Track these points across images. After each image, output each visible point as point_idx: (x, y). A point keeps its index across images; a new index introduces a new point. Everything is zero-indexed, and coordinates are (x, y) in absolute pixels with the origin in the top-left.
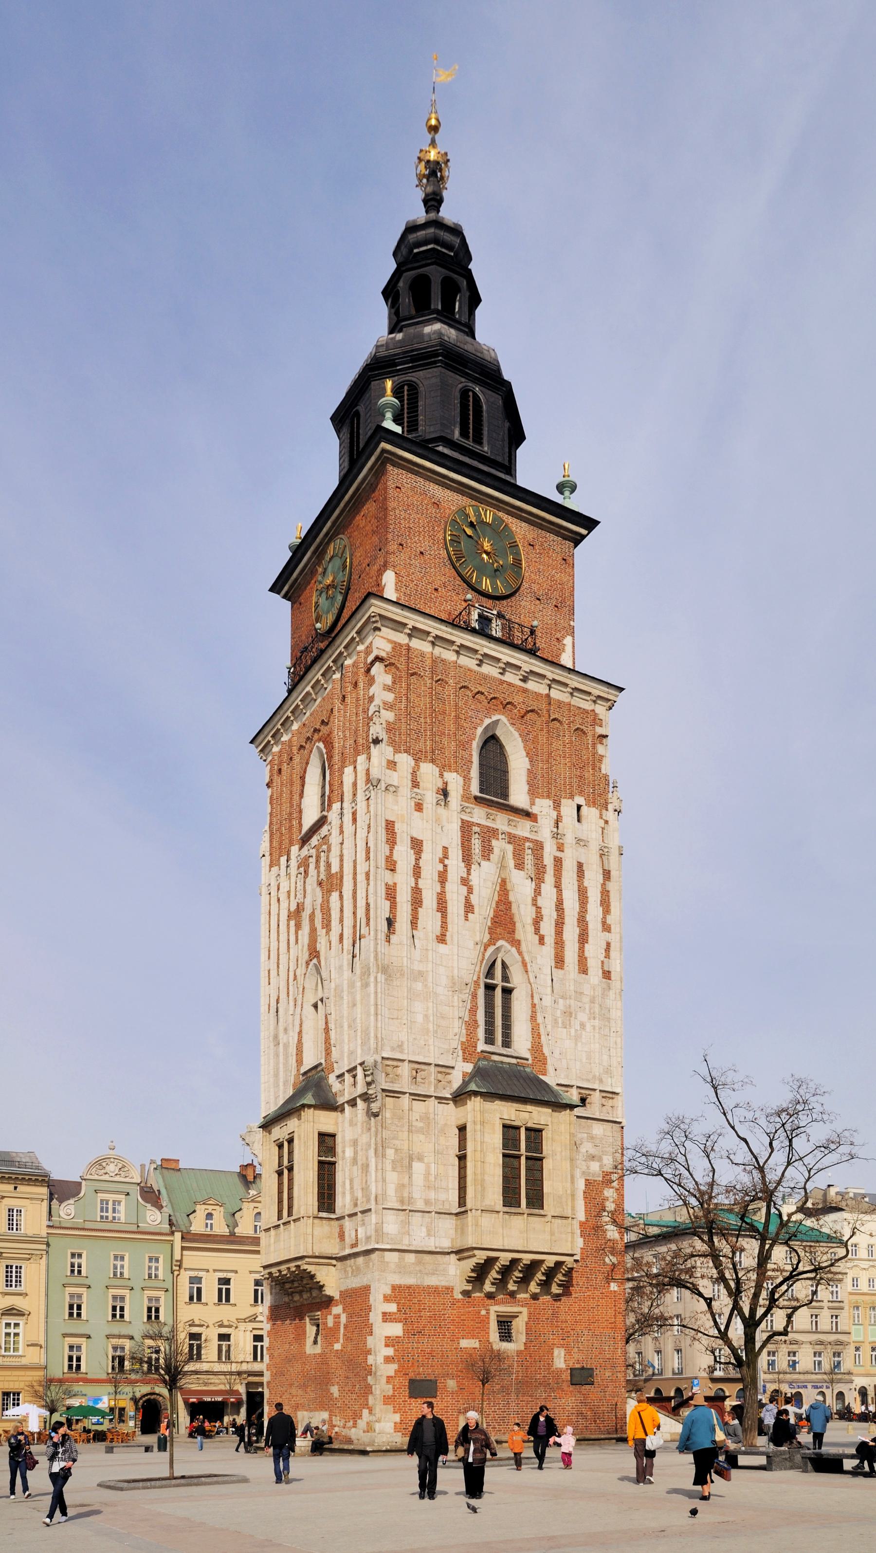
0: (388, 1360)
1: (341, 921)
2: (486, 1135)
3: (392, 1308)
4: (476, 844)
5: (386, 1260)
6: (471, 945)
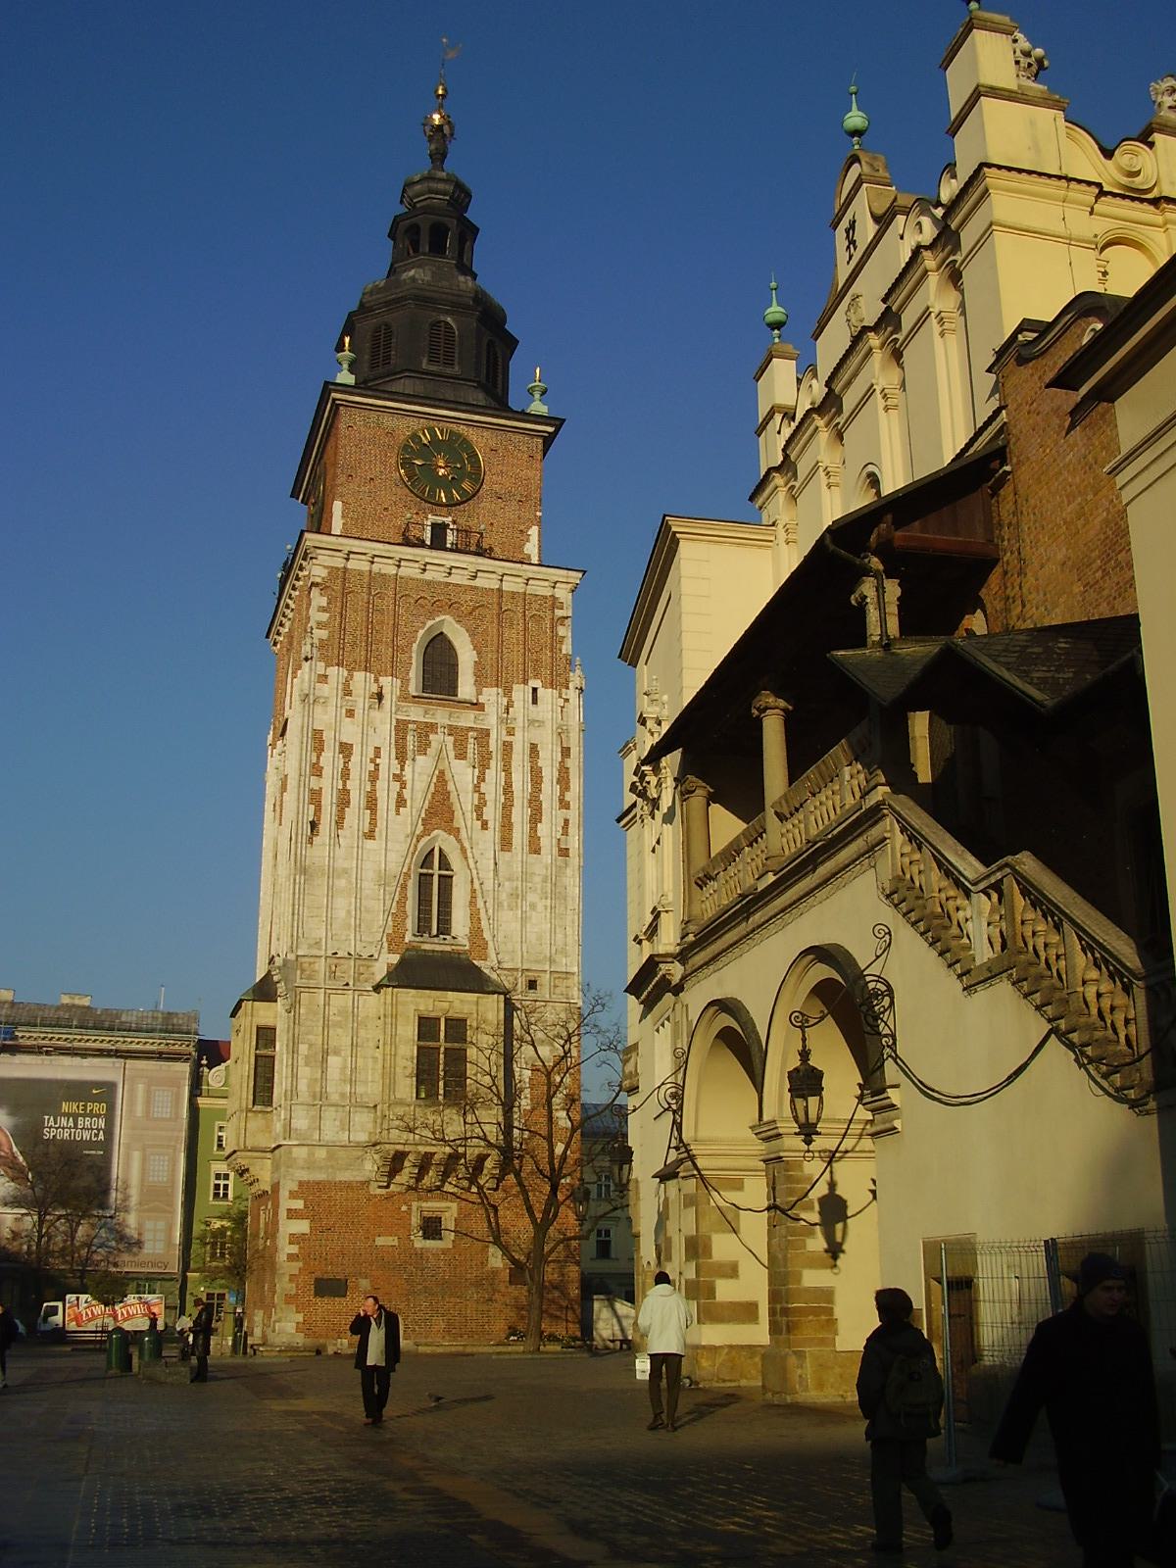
0: (291, 1257)
2: (398, 1027)
3: (299, 1204)
5: (294, 1155)
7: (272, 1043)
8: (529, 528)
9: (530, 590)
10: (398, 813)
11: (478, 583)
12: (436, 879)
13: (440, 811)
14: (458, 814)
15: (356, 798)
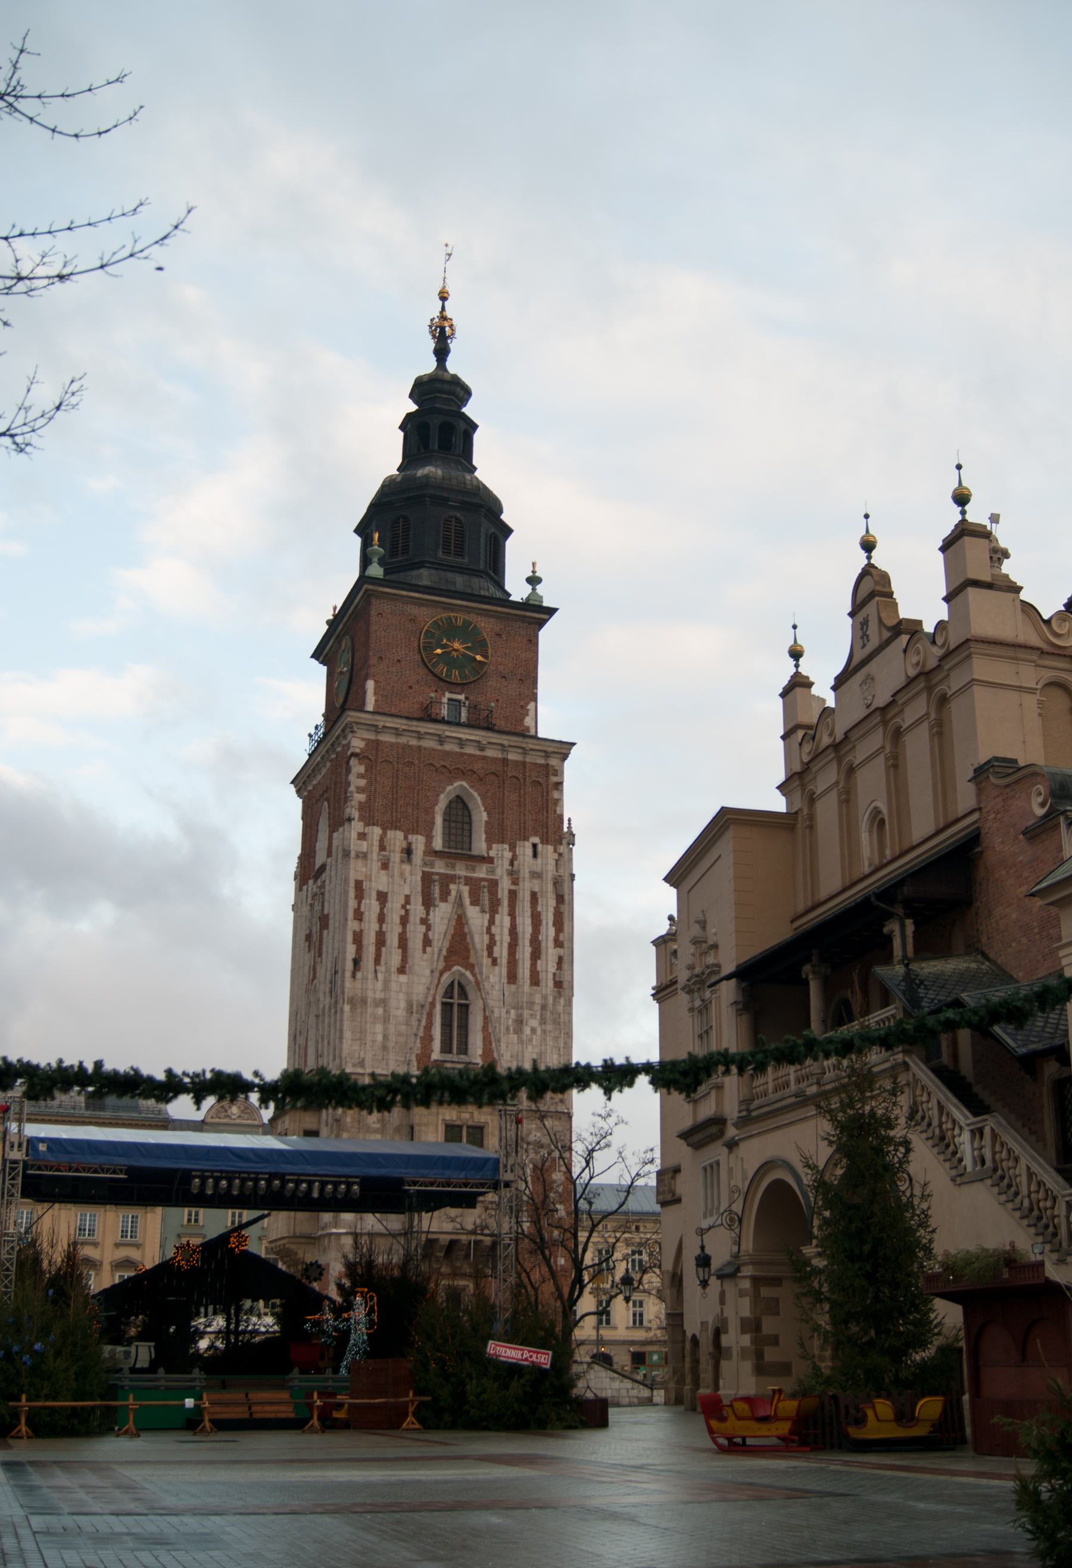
4: (436, 891)
6: (427, 972)
8: (527, 704)
9: (528, 760)
10: (424, 951)
11: (490, 753)
12: (456, 1008)
13: (459, 948)
15: (393, 940)
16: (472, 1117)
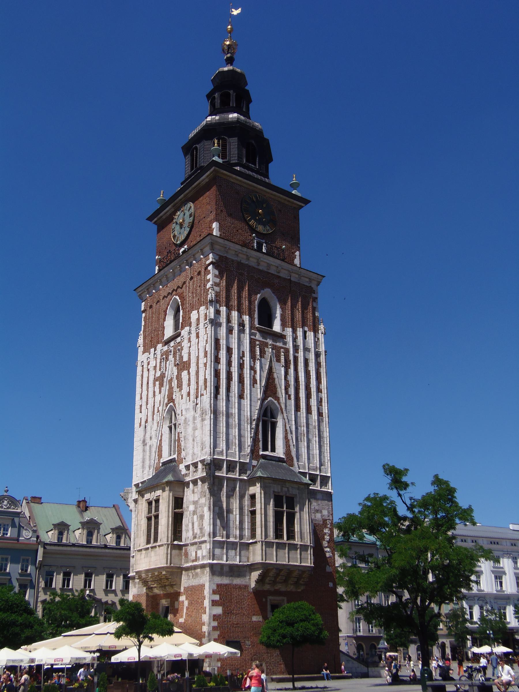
0: (214, 629)
1: (189, 385)
3: (217, 597)
7: (181, 507)
14: (279, 389)
16: (288, 490)
